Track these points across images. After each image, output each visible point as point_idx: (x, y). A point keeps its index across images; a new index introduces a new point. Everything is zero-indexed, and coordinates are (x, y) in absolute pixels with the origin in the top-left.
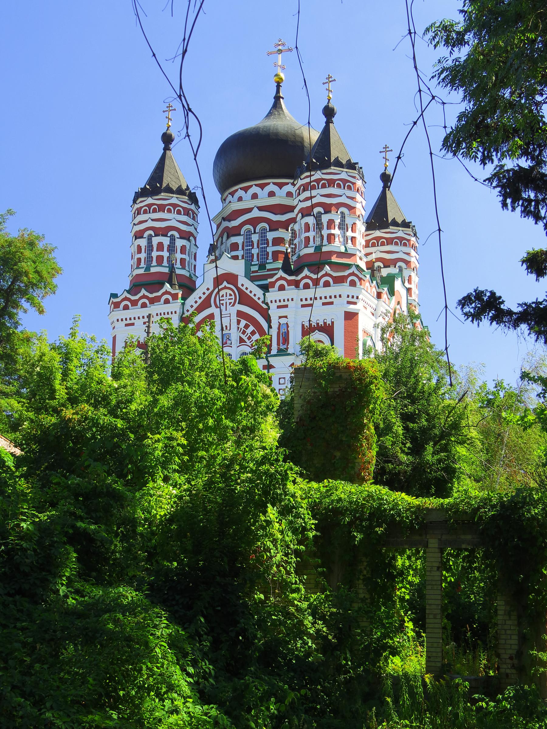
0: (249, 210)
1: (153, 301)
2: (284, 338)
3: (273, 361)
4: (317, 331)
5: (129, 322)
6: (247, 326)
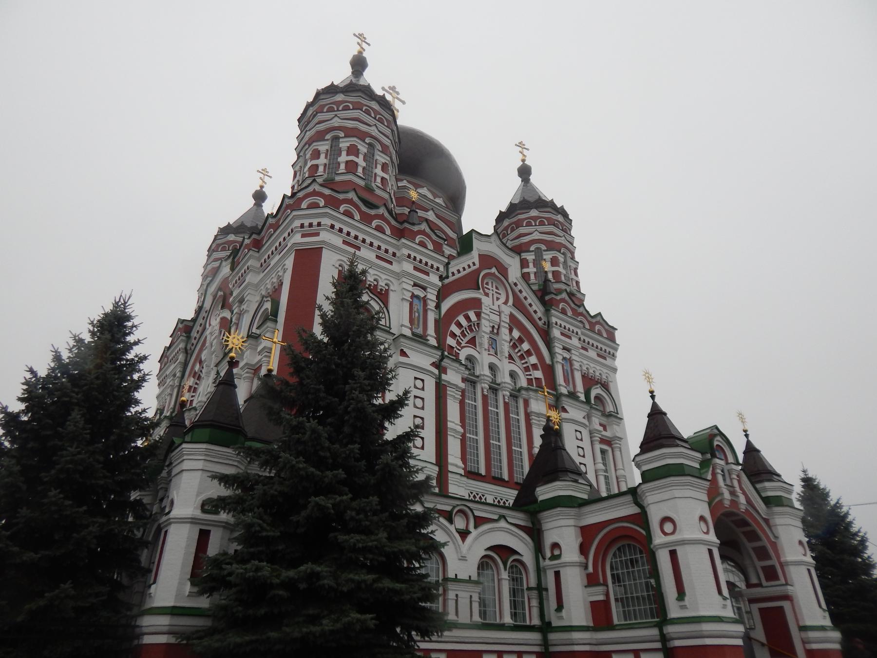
0: (427, 210)
1: (399, 234)
2: (569, 378)
3: (566, 403)
4: (599, 385)
5: (351, 239)
6: (521, 340)
